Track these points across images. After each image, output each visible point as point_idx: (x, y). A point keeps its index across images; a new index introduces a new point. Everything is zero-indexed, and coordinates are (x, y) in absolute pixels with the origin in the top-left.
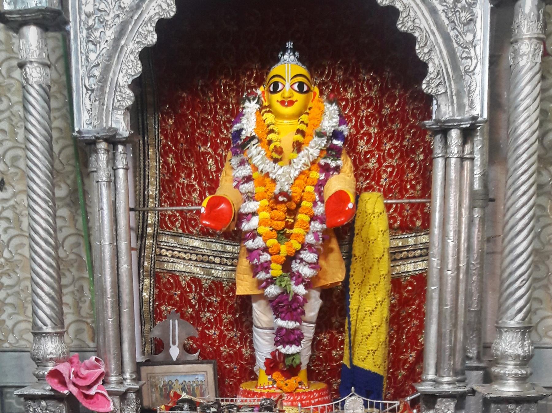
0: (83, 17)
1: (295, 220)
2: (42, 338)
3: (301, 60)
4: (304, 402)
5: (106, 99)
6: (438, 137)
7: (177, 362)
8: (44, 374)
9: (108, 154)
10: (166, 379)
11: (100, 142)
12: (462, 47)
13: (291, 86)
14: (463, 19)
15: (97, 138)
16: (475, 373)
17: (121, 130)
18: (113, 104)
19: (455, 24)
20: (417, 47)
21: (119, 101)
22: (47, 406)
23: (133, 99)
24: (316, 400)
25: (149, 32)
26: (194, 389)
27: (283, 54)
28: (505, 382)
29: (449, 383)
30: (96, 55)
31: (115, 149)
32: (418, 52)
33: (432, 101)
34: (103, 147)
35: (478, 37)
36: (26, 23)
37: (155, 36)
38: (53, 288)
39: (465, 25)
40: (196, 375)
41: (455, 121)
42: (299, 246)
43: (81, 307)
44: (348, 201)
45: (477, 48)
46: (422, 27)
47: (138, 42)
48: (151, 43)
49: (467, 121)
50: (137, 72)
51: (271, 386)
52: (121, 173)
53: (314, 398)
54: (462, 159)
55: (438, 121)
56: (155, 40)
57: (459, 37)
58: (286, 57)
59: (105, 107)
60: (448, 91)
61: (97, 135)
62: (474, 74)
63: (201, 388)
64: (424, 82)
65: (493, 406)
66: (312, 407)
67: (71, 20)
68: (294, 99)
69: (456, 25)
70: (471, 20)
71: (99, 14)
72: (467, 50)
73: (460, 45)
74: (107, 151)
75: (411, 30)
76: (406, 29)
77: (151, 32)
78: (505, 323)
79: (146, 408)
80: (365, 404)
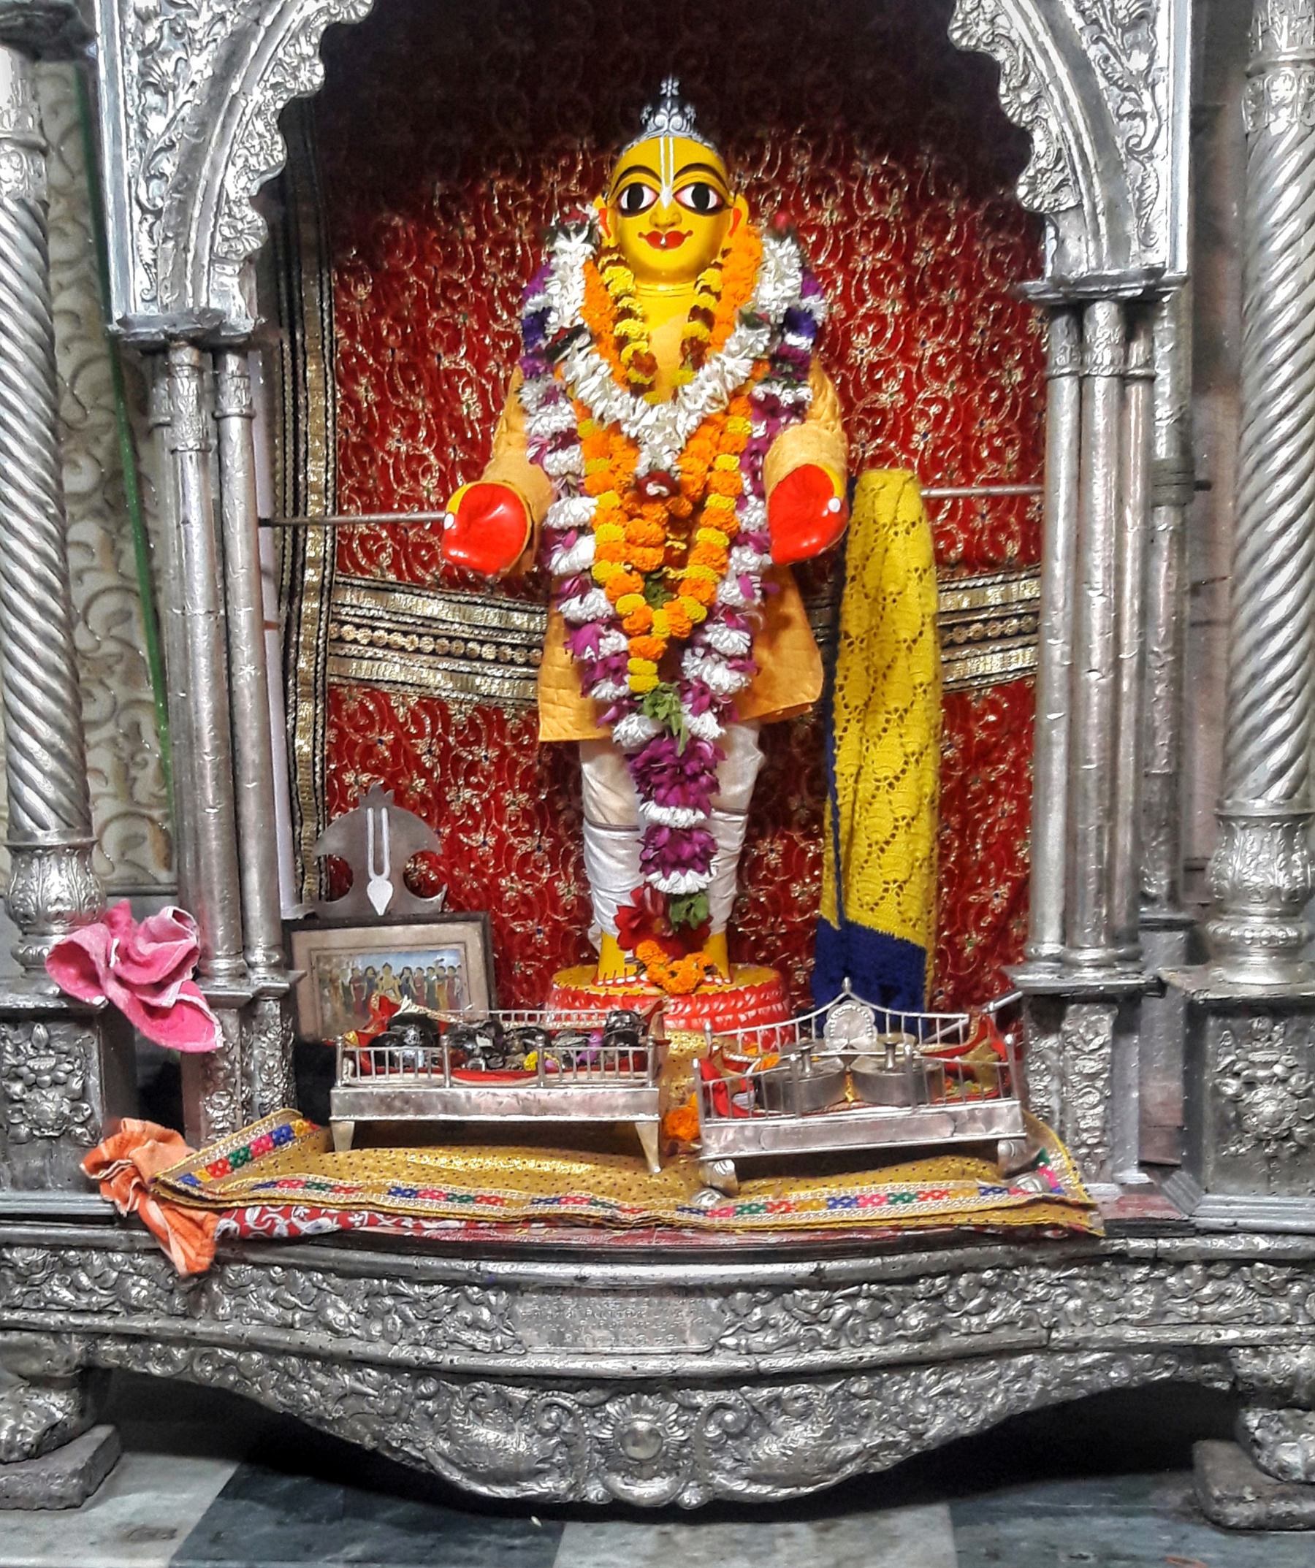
0: (131, 21)
1: (690, 544)
2: (36, 861)
3: (699, 126)
4: (718, 1019)
5: (193, 235)
7: (387, 920)
8: (40, 954)
9: (201, 379)
10: (360, 965)
12: (1120, 87)
13: (675, 195)
14: (1121, 14)
16: (1163, 937)
17: (233, 315)
19: (1101, 26)
21: (226, 239)
22: (50, 1037)
24: (752, 1013)
25: (303, 58)
26: (431, 987)
27: (654, 113)
28: (1242, 959)
29: (1098, 965)
30: (167, 121)
31: (218, 364)
32: (1004, 101)
33: (1042, 229)
35: (1161, 62)
37: (320, 69)
38: (60, 729)
39: (1126, 29)
40: (437, 952)
41: (1103, 279)
42: (701, 613)
43: (135, 779)
44: (829, 492)
45: (1160, 89)
46: (1014, 36)
47: (275, 86)
48: (309, 87)
49: (1134, 280)
51: (632, 979)
52: (234, 427)
53: (745, 1009)
55: (1058, 282)
56: (318, 81)
57: (1113, 60)
58: (661, 119)
59: (190, 256)
60: (1086, 202)
62: (1151, 158)
63: (451, 986)
64: (1022, 179)
65: (1212, 1022)
66: (740, 1031)
67: (98, 29)
68: (683, 229)
69: (1102, 30)
70: (1142, 17)
72: (1132, 95)
73: (1115, 83)
74: (198, 370)
75: (987, 44)
76: (973, 42)
77: (309, 58)
78: (1242, 805)
79: (308, 1040)
80: (880, 1023)
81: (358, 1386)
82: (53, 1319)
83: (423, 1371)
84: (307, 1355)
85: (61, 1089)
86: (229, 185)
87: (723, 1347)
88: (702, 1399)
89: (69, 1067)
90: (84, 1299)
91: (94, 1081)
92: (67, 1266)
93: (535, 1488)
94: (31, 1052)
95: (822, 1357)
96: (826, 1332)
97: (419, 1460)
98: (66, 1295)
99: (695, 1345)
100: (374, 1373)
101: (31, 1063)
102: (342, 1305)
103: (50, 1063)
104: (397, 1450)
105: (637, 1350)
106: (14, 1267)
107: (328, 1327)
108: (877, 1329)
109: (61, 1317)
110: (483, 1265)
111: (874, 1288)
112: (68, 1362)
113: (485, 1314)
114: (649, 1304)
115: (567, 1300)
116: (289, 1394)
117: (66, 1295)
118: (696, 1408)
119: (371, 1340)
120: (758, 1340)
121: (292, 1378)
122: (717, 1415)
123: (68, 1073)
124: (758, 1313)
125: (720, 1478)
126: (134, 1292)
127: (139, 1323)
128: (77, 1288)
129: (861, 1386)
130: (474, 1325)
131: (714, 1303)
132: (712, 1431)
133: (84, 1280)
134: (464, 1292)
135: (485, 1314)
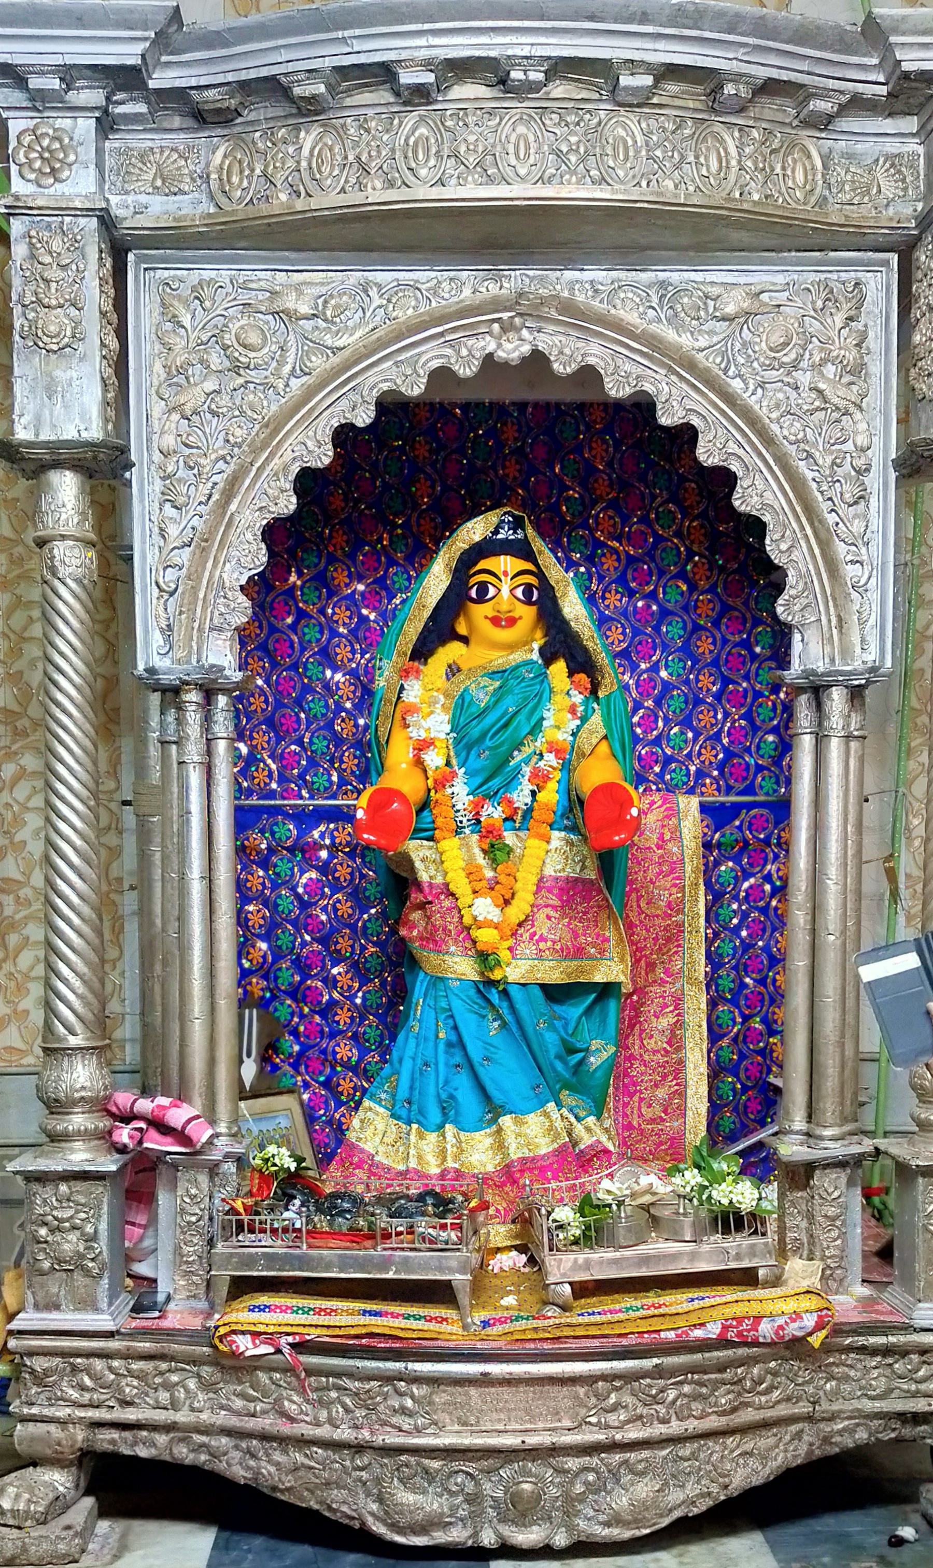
0: (157, 457)
2: (66, 1059)
5: (199, 610)
6: (803, 699)
11: (189, 691)
14: (847, 496)
15: (188, 683)
18: (211, 620)
20: (767, 541)
22: (71, 1193)
23: (250, 611)
32: (768, 548)
34: (194, 700)
35: (873, 526)
36: (57, 465)
37: (294, 499)
38: (87, 962)
39: (850, 506)
45: (873, 547)
47: (260, 509)
48: (286, 511)
50: (258, 563)
54: (848, 737)
56: (293, 507)
57: (841, 525)
59: (196, 625)
60: (823, 618)
61: (186, 678)
71: (187, 451)
72: (854, 548)
81: (307, 1461)
82: (62, 1412)
83: (359, 1448)
84: (264, 1437)
85: (78, 1233)
86: (225, 576)
87: (590, 1423)
88: (572, 1463)
89: (83, 1215)
90: (87, 1396)
91: (103, 1226)
92: (75, 1369)
93: (440, 1537)
94: (55, 1204)
95: (658, 1430)
96: (662, 1410)
97: (354, 1518)
98: (74, 1394)
99: (567, 1423)
100: (320, 1451)
101: (55, 1213)
102: (295, 1398)
103: (70, 1212)
104: (335, 1511)
105: (523, 1427)
106: (33, 1372)
107: (284, 1414)
108: (697, 1407)
109: (68, 1411)
110: (411, 1366)
111: (696, 1377)
112: (72, 1446)
113: (409, 1403)
114: (534, 1393)
115: (473, 1391)
116: (248, 1468)
117: (74, 1394)
118: (567, 1471)
119: (318, 1424)
120: (612, 1419)
121: (253, 1456)
122: (582, 1477)
123: (82, 1220)
124: (613, 1398)
125: (582, 1524)
126: (127, 1390)
127: (130, 1415)
128: (83, 1388)
129: (686, 1450)
130: (404, 1411)
131: (581, 1391)
132: (579, 1488)
133: (87, 1381)
134: (394, 1385)
135: (409, 1403)
